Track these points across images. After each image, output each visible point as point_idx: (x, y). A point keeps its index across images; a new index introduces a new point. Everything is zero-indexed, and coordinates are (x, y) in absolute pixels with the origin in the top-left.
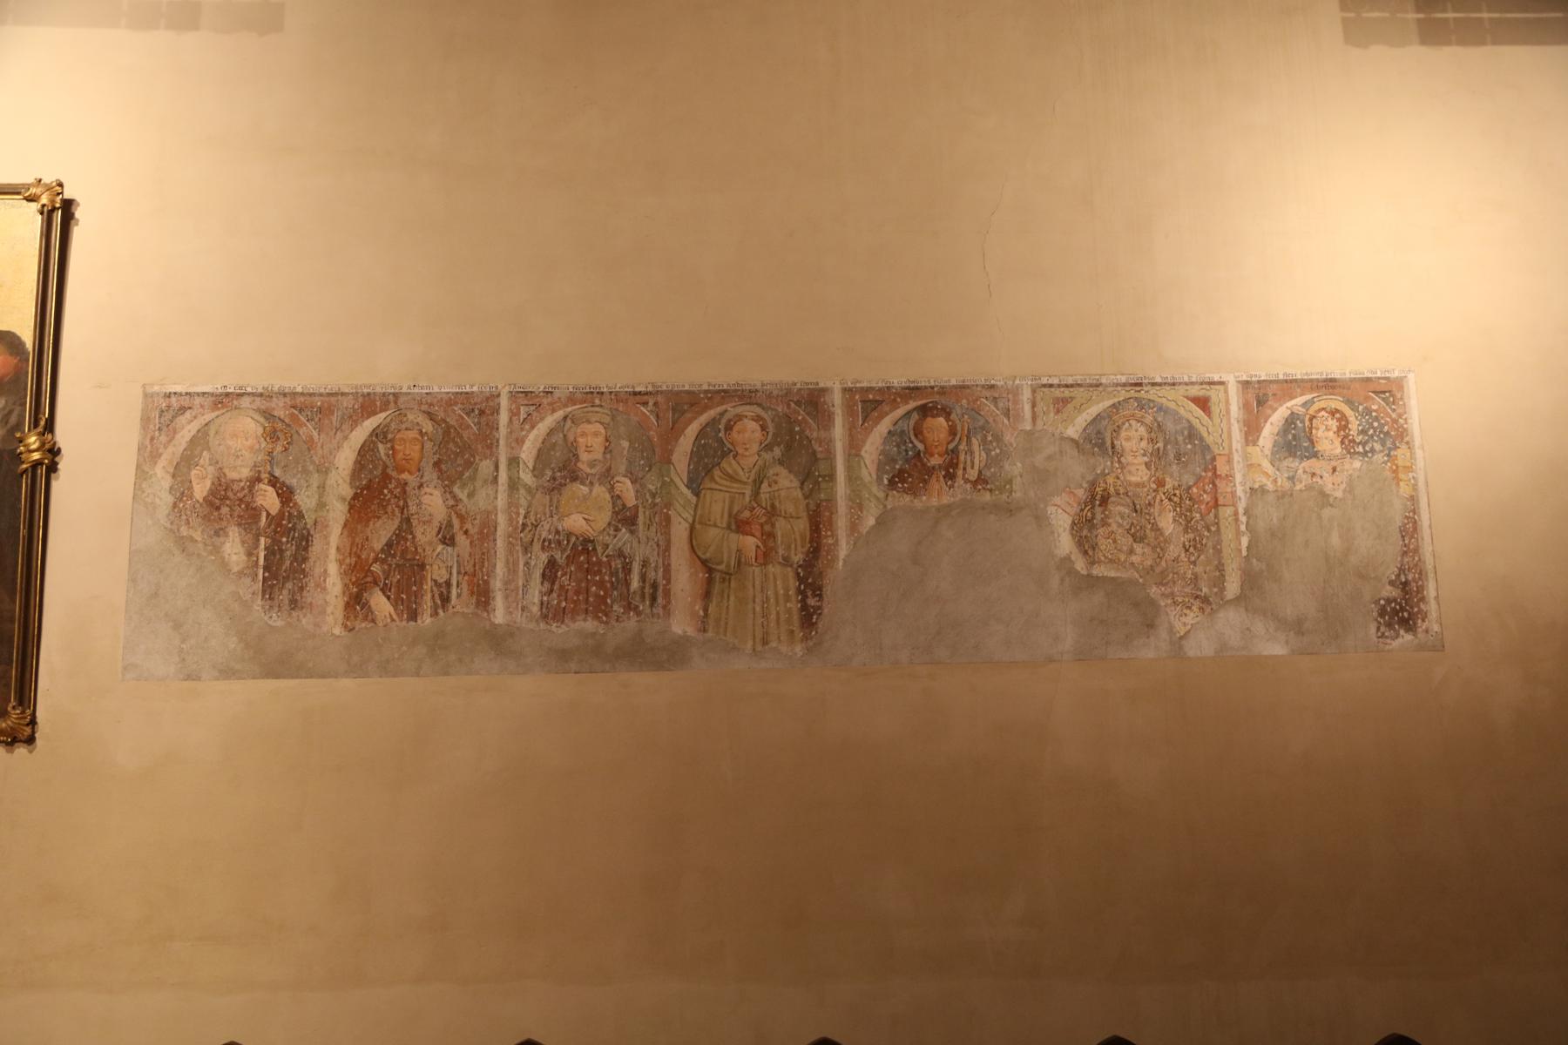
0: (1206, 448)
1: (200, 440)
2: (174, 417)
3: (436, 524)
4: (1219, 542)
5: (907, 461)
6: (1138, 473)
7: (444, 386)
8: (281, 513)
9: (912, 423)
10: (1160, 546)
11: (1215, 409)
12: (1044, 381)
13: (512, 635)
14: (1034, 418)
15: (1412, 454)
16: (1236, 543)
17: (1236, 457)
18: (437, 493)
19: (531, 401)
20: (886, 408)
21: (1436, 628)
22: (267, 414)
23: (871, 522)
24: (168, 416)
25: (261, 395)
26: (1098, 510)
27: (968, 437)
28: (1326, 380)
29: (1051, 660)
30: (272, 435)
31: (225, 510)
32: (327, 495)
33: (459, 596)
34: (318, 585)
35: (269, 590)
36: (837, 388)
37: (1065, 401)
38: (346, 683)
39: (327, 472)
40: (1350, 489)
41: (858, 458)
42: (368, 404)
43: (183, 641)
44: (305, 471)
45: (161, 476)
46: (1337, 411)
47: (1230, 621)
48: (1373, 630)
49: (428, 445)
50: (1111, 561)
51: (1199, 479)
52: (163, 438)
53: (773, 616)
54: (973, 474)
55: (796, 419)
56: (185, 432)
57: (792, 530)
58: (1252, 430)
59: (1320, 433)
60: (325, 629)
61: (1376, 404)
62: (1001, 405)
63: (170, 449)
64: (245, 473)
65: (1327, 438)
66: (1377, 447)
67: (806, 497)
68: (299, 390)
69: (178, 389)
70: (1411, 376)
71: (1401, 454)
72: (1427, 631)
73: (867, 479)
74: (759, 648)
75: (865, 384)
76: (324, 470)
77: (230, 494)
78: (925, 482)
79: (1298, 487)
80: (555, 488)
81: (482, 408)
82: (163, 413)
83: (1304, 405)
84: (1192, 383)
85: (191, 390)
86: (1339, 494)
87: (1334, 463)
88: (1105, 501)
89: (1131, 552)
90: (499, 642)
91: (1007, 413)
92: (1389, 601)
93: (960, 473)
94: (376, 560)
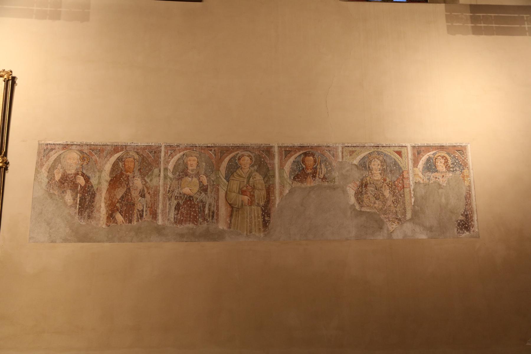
1: (58, 160)
2: (49, 152)
3: (139, 190)
4: (404, 200)
5: (299, 171)
6: (377, 177)
7: (142, 143)
8: (85, 185)
9: (301, 158)
10: (385, 201)
11: (403, 155)
12: (346, 145)
13: (164, 228)
14: (343, 157)
15: (469, 172)
16: (410, 200)
17: (410, 172)
18: (139, 179)
19: (172, 149)
20: (293, 153)
21: (477, 230)
22: (81, 152)
23: (287, 191)
24: (47, 151)
25: (79, 145)
26: (364, 189)
27: (320, 164)
28: (440, 146)
29: (347, 239)
30: (83, 159)
31: (66, 184)
32: (101, 180)
33: (146, 215)
34: (97, 211)
35: (80, 212)
36: (276, 146)
37: (353, 152)
38: (107, 244)
39: (101, 172)
40: (448, 183)
41: (283, 170)
42: (116, 149)
43: (50, 229)
44: (94, 171)
45: (44, 172)
46: (444, 156)
47: (408, 227)
48: (456, 230)
49: (137, 163)
50: (368, 206)
51: (398, 179)
52: (45, 159)
53: (253, 223)
54: (322, 176)
55: (262, 156)
56: (53, 157)
58: (416, 163)
59: (438, 164)
60: (100, 225)
61: (457, 154)
62: (331, 153)
63: (47, 163)
64: (73, 171)
65: (441, 165)
66: (458, 169)
67: (265, 183)
68: (92, 143)
69: (51, 142)
70: (469, 145)
71: (466, 171)
72: (474, 231)
73: (286, 177)
74: (248, 234)
75: (285, 145)
76: (100, 171)
77: (68, 179)
78: (306, 178)
80: (180, 178)
81: (155, 151)
82: (45, 150)
84: (396, 146)
86: (445, 185)
87: (443, 174)
88: (366, 186)
89: (375, 203)
90: (160, 231)
91: (334, 156)
92: (461, 221)
93: (317, 175)
94: (118, 202)
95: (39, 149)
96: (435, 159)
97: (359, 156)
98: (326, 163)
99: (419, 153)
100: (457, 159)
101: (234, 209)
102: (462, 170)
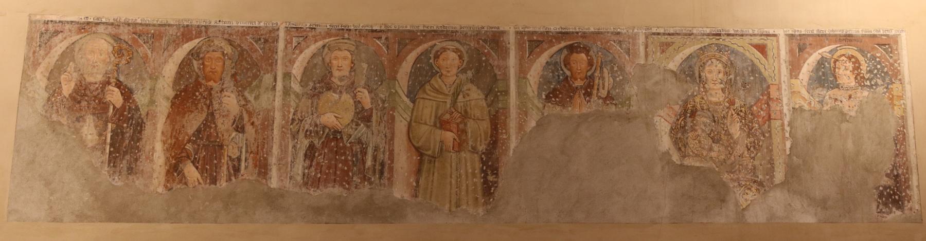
0: (764, 80)
1: (68, 54)
2: (50, 38)
3: (232, 117)
4: (771, 144)
5: (559, 82)
7: (240, 21)
8: (123, 106)
9: (563, 57)
10: (730, 146)
11: (770, 53)
12: (654, 30)
13: (282, 196)
14: (646, 56)
15: (903, 88)
16: (782, 145)
17: (784, 86)
18: (233, 96)
19: (301, 34)
20: (545, 46)
21: (917, 207)
22: (116, 38)
23: (533, 124)
24: (46, 37)
25: (112, 24)
26: (689, 120)
27: (601, 68)
28: (846, 35)
29: (653, 222)
30: (119, 52)
31: (84, 103)
32: (156, 94)
33: (246, 167)
34: (147, 158)
35: (113, 160)
36: (512, 31)
37: (668, 45)
38: (166, 227)
39: (157, 79)
40: (861, 110)
41: (523, 80)
42: (187, 32)
43: (51, 194)
44: (141, 78)
45: (40, 78)
46: (853, 57)
47: (777, 199)
48: (874, 206)
49: (228, 63)
50: (697, 155)
51: (759, 100)
52: (42, 52)
53: (464, 187)
54: (604, 93)
55: (483, 52)
56: (58, 47)
57: (478, 128)
58: (795, 68)
59: (841, 72)
60: (152, 188)
61: (879, 52)
62: (624, 46)
63: (47, 60)
64: (99, 78)
65: (845, 75)
66: (880, 82)
67: (489, 106)
68: (139, 21)
69: (54, 18)
70: (903, 34)
71: (896, 87)
72: (911, 209)
73: (531, 94)
74: (454, 209)
75: (531, 29)
76: (154, 78)
77: (88, 92)
78: (571, 98)
79: (825, 108)
80: (315, 95)
81: (267, 38)
83: (831, 52)
84: (755, 35)
85: (62, 19)
86: (853, 114)
87: (850, 92)
88: (693, 114)
89: (711, 149)
90: (274, 201)
91: (628, 52)
92: (885, 188)
93: (595, 92)
94: (189, 141)
95: (30, 32)
96: (835, 62)
97: (681, 54)
98: (612, 68)
99: (801, 50)
100: (879, 63)
101: (424, 158)
102: (888, 84)
